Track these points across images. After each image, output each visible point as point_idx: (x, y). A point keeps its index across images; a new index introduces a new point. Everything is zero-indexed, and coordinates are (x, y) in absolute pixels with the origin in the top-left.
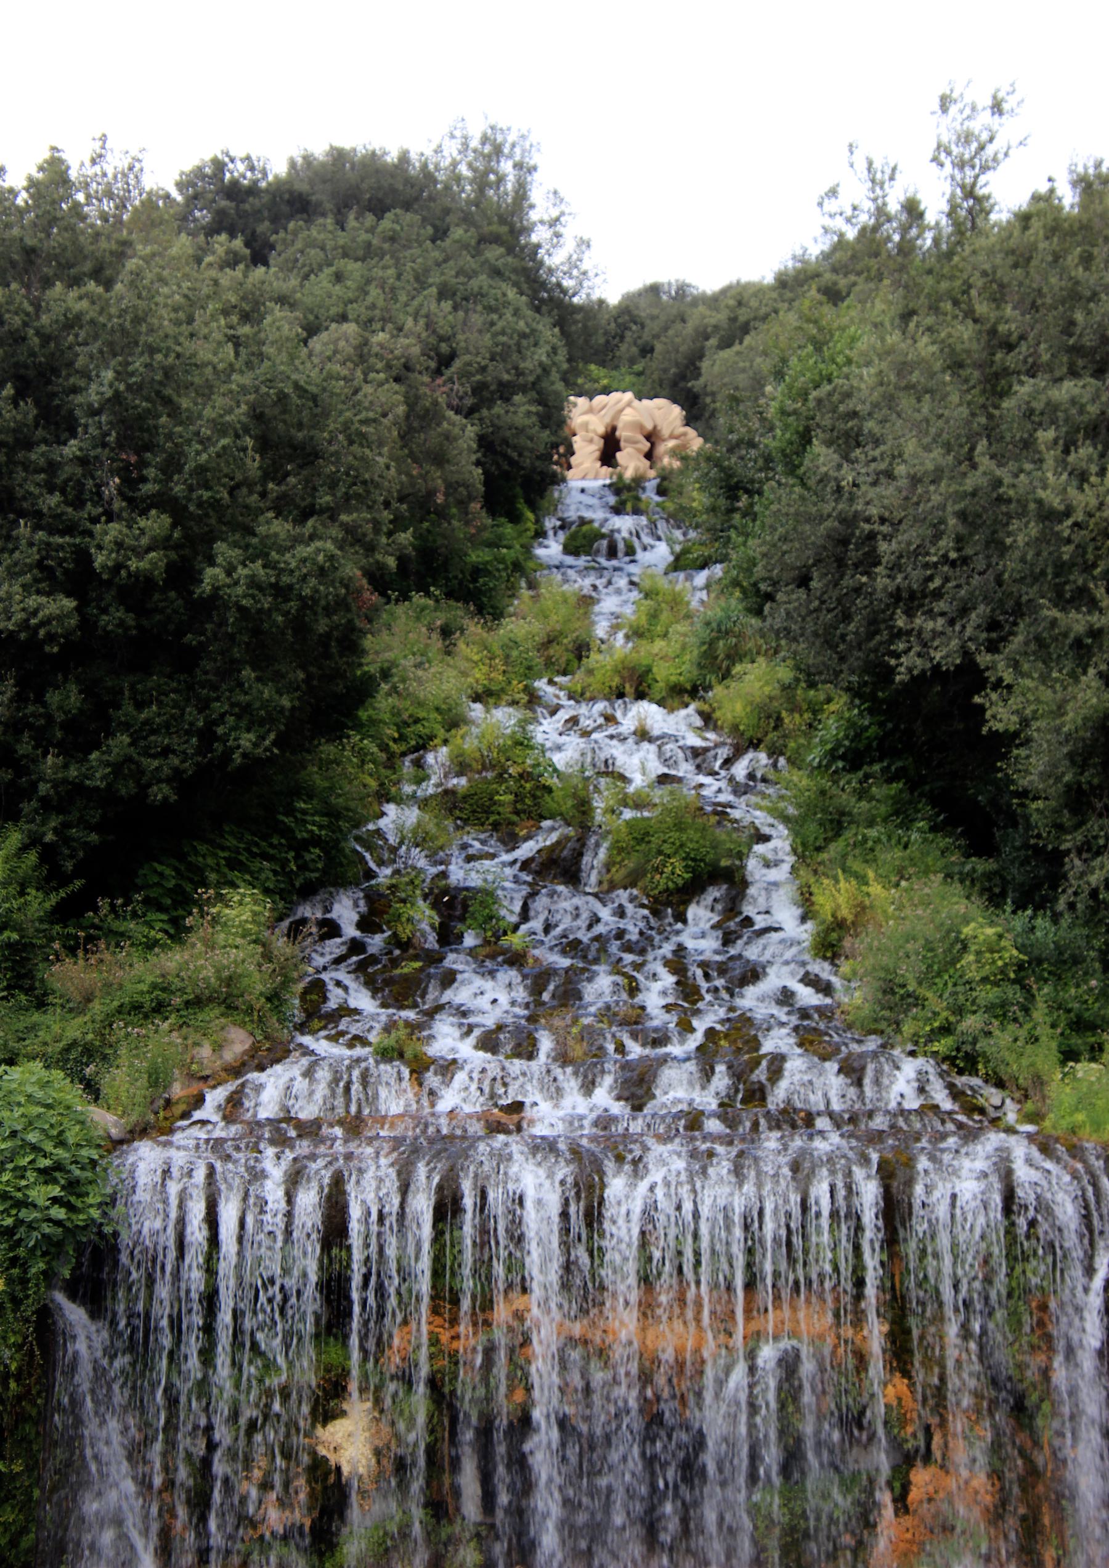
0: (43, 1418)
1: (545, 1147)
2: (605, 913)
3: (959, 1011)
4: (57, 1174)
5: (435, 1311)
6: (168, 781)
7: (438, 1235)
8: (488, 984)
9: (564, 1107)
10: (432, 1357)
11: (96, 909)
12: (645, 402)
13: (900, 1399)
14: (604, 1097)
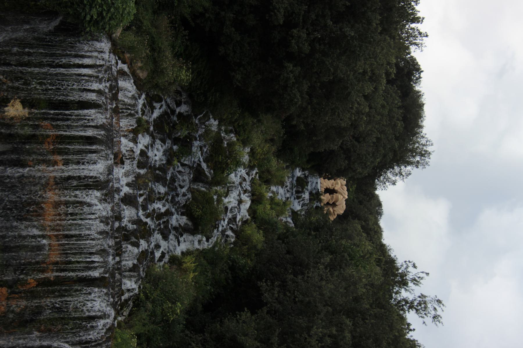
1: (110, 171)
2: (184, 190)
3: (153, 302)
4: (100, 18)
5: (57, 137)
7: (81, 137)
8: (161, 153)
9: (122, 177)
10: (42, 135)
11: (185, 30)
12: (344, 202)
13: (29, 284)
14: (126, 190)
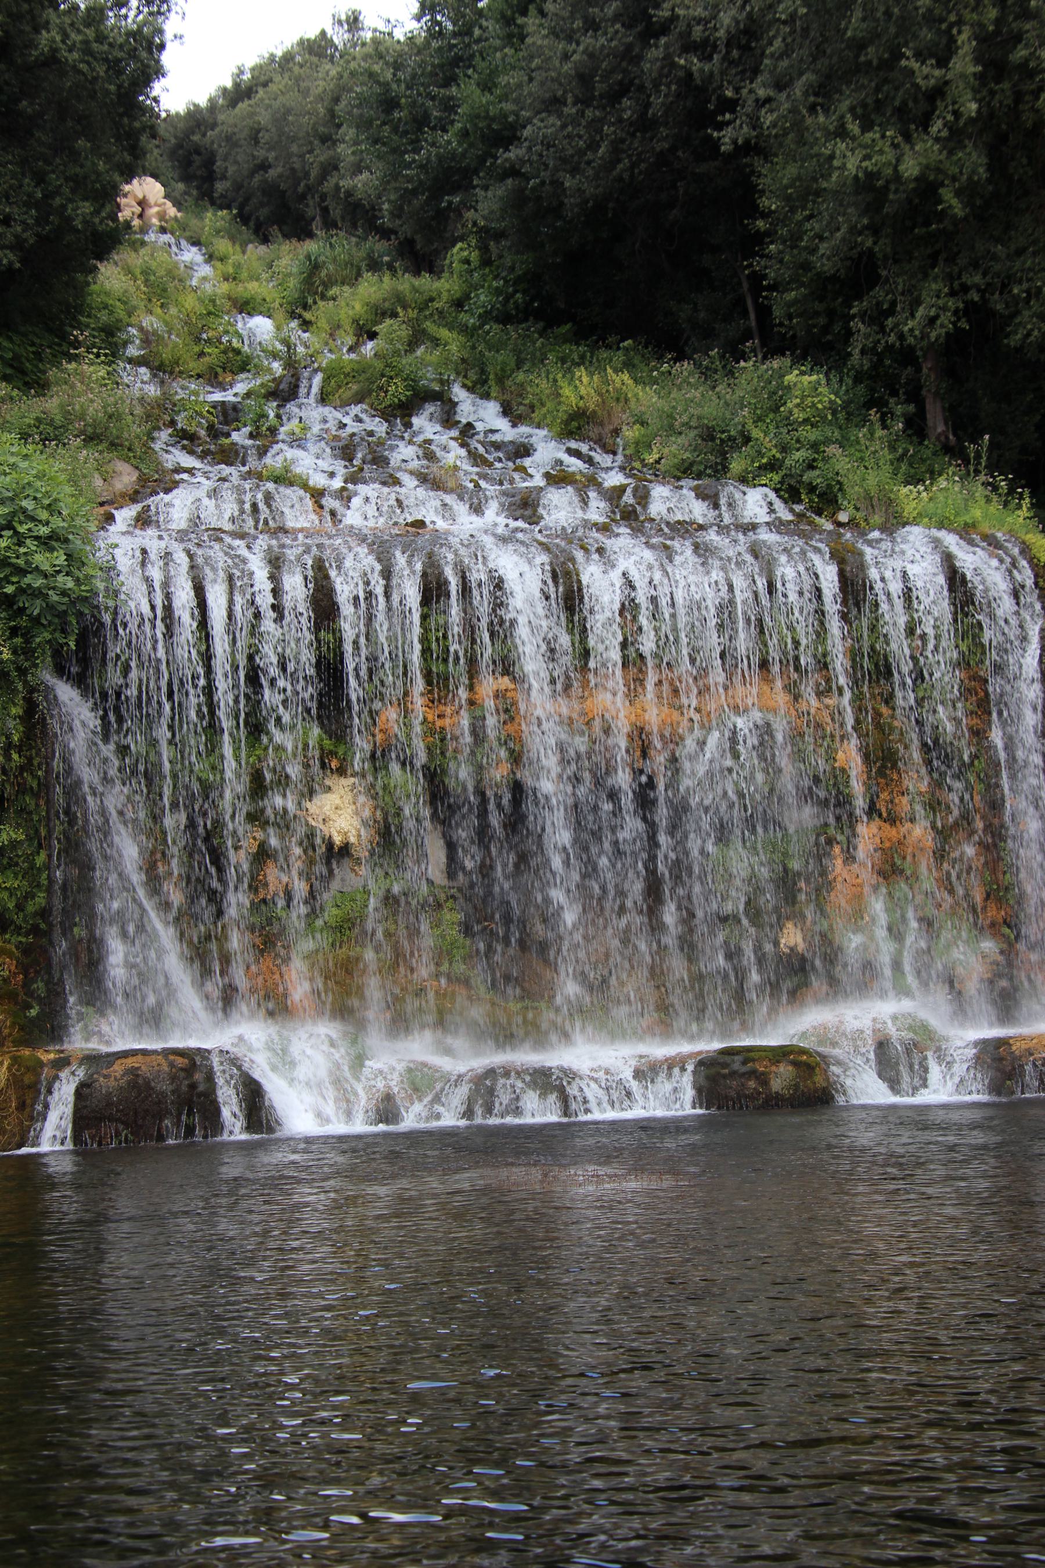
0: (45, 788)
3: (784, 449)
6: (11, 248)
